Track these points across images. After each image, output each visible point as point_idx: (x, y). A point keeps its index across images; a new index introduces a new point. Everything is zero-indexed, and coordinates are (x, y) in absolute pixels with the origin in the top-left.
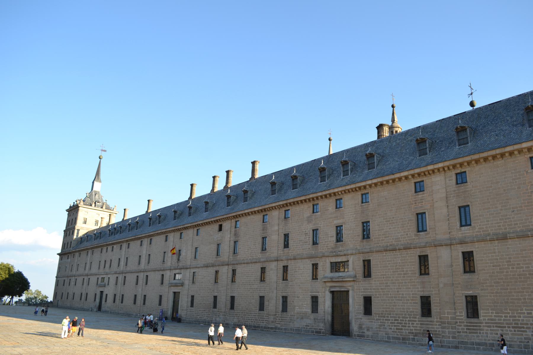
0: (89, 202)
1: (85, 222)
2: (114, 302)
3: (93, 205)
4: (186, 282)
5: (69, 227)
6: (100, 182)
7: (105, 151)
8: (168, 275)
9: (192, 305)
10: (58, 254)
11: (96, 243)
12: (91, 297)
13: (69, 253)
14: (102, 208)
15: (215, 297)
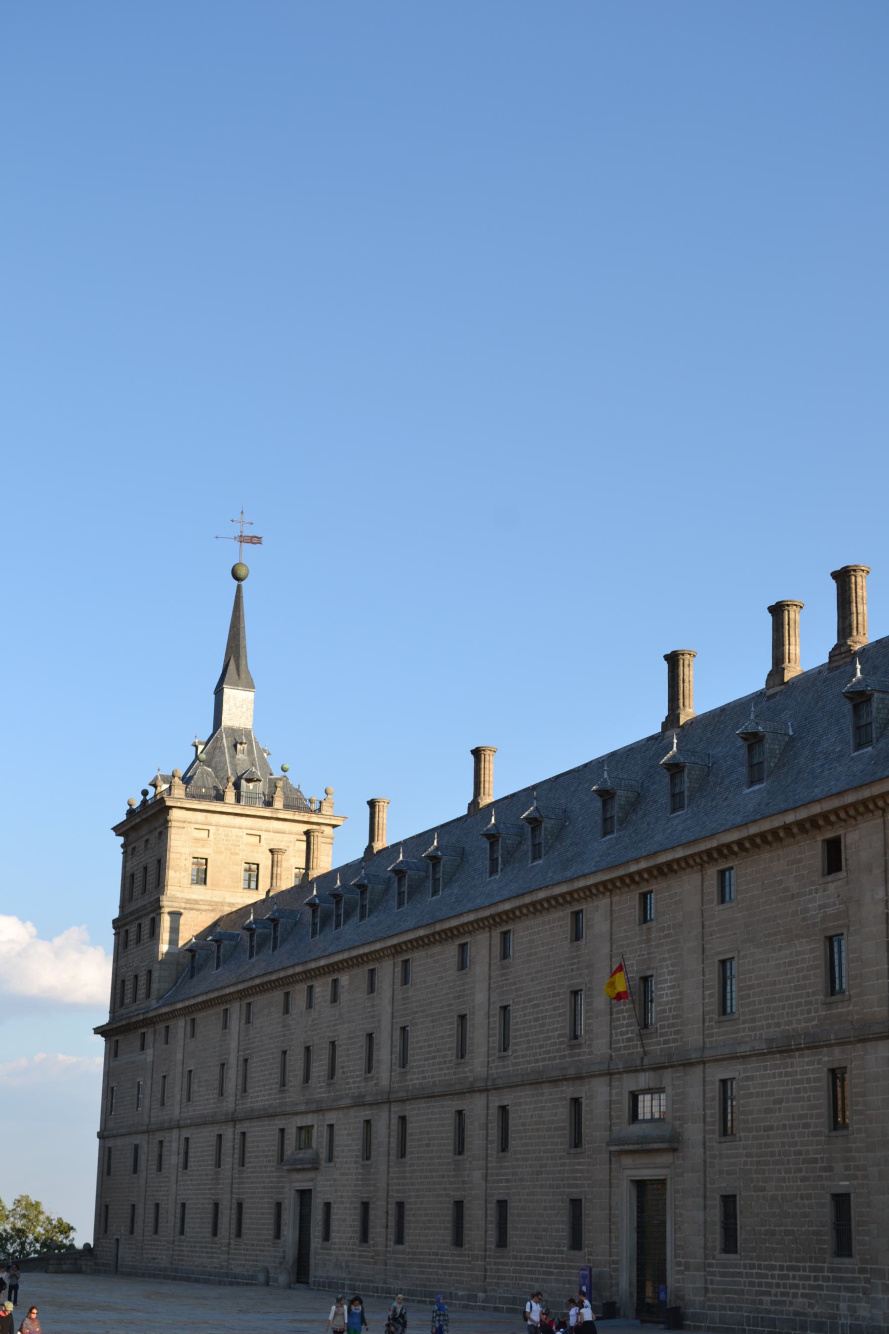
0: (210, 782)
1: (201, 878)
2: (364, 1237)
3: (230, 795)
4: (693, 1132)
5: (134, 906)
6: (249, 685)
7: (255, 540)
8: (599, 1096)
9: (730, 1244)
10: (98, 1031)
11: (257, 968)
12: (258, 1219)
13: (149, 1022)
14: (269, 804)
15: (841, 1202)
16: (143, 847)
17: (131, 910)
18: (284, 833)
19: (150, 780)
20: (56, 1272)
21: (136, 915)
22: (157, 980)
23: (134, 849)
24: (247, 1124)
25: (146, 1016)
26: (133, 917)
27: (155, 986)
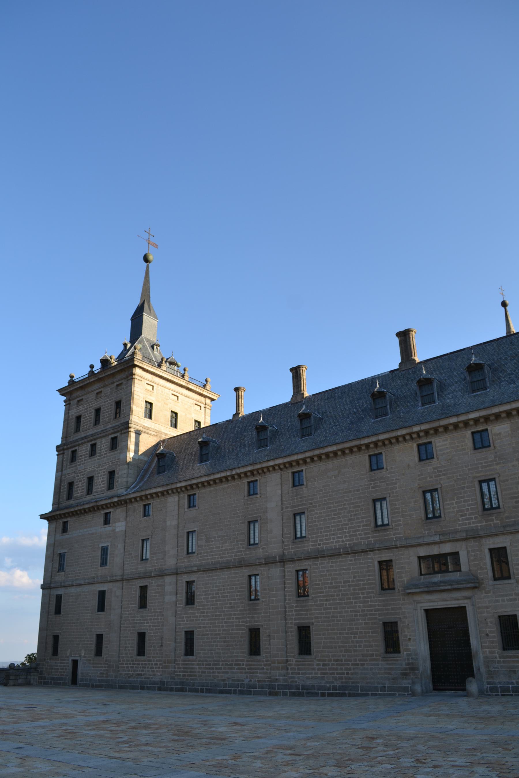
5: (81, 434)
6: (156, 317)
7: (156, 246)
10: (43, 517)
16: (94, 397)
17: (75, 438)
18: (189, 398)
19: (101, 357)
20: (14, 685)
21: (89, 439)
22: (125, 475)
23: (78, 401)
24: (310, 562)
25: (123, 498)
26: (85, 440)
27: (121, 479)
